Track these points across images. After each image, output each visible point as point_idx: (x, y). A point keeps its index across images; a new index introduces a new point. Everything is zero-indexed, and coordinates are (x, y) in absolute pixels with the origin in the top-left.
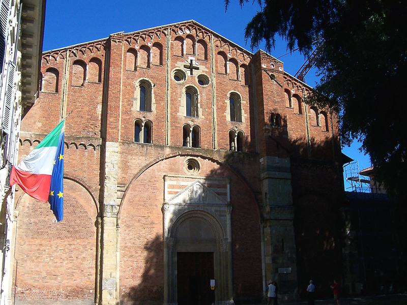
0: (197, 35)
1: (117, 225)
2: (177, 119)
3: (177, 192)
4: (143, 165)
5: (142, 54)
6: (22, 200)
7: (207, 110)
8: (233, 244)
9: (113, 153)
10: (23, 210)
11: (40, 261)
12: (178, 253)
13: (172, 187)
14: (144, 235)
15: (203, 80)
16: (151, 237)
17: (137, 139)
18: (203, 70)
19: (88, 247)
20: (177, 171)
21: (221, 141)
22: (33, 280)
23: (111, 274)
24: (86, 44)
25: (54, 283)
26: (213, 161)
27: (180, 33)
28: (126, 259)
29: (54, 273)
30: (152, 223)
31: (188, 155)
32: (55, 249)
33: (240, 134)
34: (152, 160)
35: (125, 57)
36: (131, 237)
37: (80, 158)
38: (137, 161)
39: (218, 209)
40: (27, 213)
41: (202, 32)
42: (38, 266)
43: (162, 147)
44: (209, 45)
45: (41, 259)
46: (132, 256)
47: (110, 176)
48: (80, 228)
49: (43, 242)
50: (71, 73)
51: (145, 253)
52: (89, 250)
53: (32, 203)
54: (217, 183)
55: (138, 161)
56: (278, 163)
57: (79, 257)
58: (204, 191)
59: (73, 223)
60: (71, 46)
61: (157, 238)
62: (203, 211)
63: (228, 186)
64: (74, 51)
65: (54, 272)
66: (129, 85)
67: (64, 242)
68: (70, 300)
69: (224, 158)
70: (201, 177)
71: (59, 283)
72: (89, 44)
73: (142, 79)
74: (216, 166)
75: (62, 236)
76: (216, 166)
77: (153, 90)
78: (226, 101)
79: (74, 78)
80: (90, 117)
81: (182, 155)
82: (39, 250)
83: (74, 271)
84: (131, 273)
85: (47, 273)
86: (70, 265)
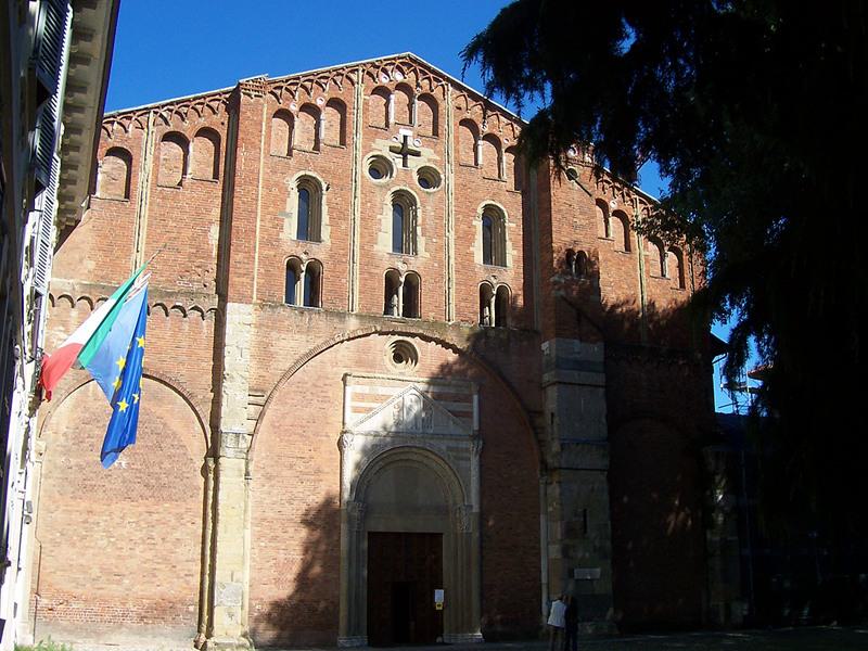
0: (418, 85)
1: (247, 474)
3: (371, 409)
5: (303, 122)
6: (54, 420)
7: (434, 240)
8: (483, 517)
9: (240, 327)
10: (56, 440)
12: (369, 533)
13: (361, 397)
14: (301, 495)
15: (428, 178)
16: (317, 499)
17: (290, 298)
18: (428, 157)
19: (187, 518)
20: (371, 365)
21: (463, 304)
22: (74, 584)
24: (189, 100)
26: (446, 345)
27: (383, 80)
28: (263, 544)
29: (116, 570)
30: (318, 471)
31: (393, 333)
32: (119, 520)
33: (502, 290)
35: (269, 127)
36: (274, 499)
37: (174, 335)
38: (291, 344)
39: (452, 444)
40: (65, 447)
41: (429, 78)
42: (83, 555)
43: (342, 316)
44: (442, 106)
46: (274, 539)
47: (234, 374)
48: (171, 478)
50: (157, 158)
51: (304, 533)
52: (189, 524)
53: (72, 425)
54: (453, 391)
55: (293, 343)
56: (579, 353)
58: (425, 408)
59: (157, 469)
60: (157, 104)
61: (328, 502)
62: (423, 449)
63: (476, 397)
64: (165, 114)
65: (116, 567)
68: (149, 626)
69: (468, 340)
70: (421, 379)
71: (127, 590)
72: (195, 99)
73: (302, 173)
74: (451, 357)
76: (451, 357)
77: (324, 198)
78: (474, 223)
79: (163, 170)
80: (194, 251)
81: (381, 333)
82: (86, 522)
83: (158, 566)
84: (273, 573)
85: (102, 570)
86: (149, 555)
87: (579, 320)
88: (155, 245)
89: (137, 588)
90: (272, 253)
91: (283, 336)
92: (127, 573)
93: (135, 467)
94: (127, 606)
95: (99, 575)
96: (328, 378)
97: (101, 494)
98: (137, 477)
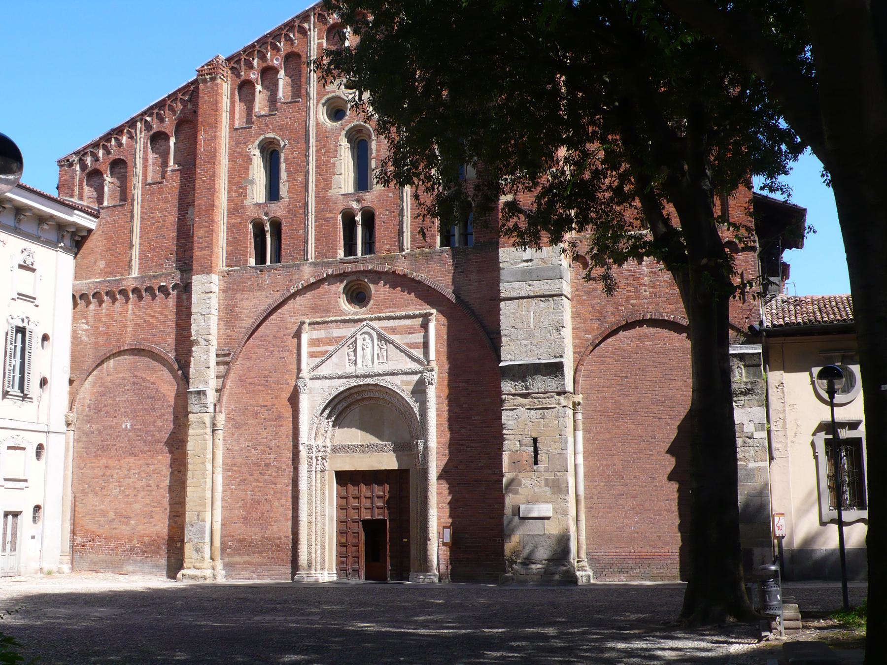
2: (328, 200)
4: (263, 308)
10: (83, 411)
11: (105, 493)
13: (314, 342)
22: (97, 525)
23: (198, 515)
25: (125, 530)
28: (233, 487)
32: (126, 473)
34: (278, 294)
40: (87, 416)
42: (103, 502)
45: (107, 491)
46: (242, 482)
49: (110, 463)
55: (255, 301)
57: (160, 486)
59: (152, 428)
65: (126, 511)
66: (241, 155)
67: (139, 460)
68: (149, 559)
71: (133, 529)
75: (136, 451)
77: (282, 155)
82: (104, 475)
83: (154, 509)
85: (116, 513)
88: (146, 236)
89: (140, 527)
90: (238, 220)
91: (246, 296)
92: (132, 515)
93: (137, 427)
94: (133, 543)
95: (114, 517)
96: (286, 328)
97: (113, 452)
98: (138, 436)
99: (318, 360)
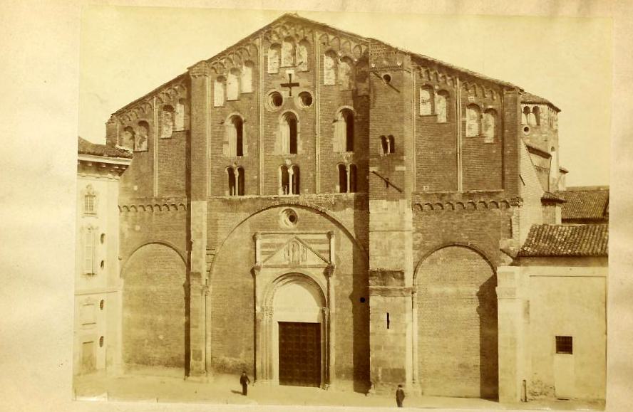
3: (269, 253)
13: (264, 246)
38: (228, 219)
87: (387, 186)
99: (266, 256)
